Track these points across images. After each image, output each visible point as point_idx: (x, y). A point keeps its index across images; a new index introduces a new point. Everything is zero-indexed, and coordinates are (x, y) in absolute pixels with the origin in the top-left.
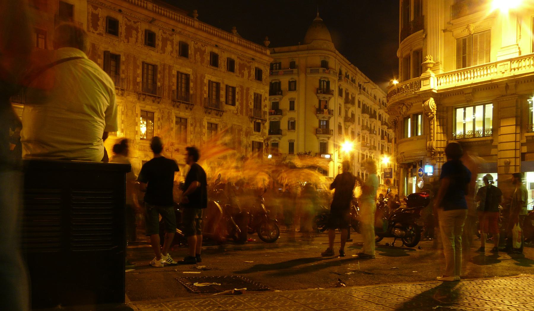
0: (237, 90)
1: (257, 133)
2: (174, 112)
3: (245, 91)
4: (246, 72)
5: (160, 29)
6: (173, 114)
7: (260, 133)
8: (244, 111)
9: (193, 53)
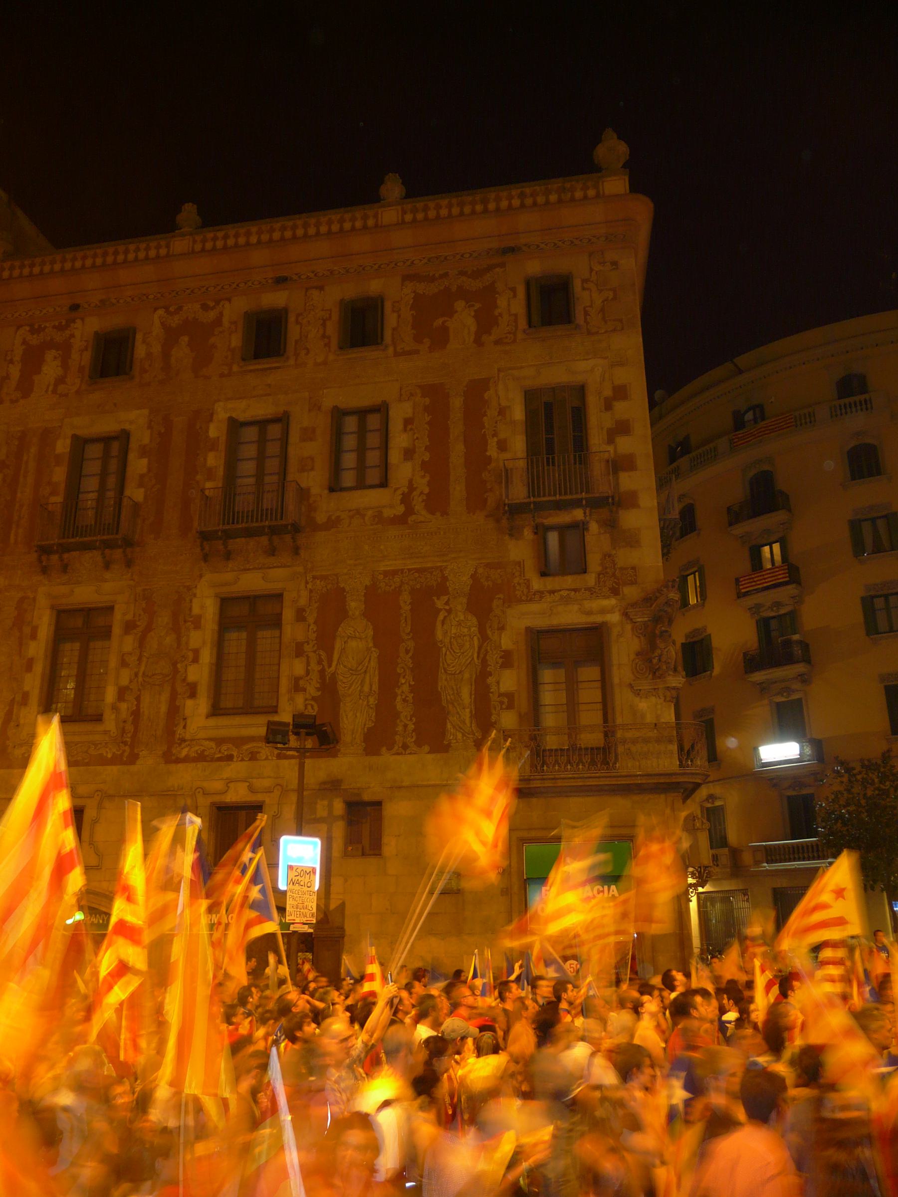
0: (399, 413)
1: (569, 581)
2: (45, 598)
3: (457, 403)
4: (463, 321)
5: (19, 327)
6: (43, 602)
7: (590, 579)
8: (458, 490)
9: (157, 349)
